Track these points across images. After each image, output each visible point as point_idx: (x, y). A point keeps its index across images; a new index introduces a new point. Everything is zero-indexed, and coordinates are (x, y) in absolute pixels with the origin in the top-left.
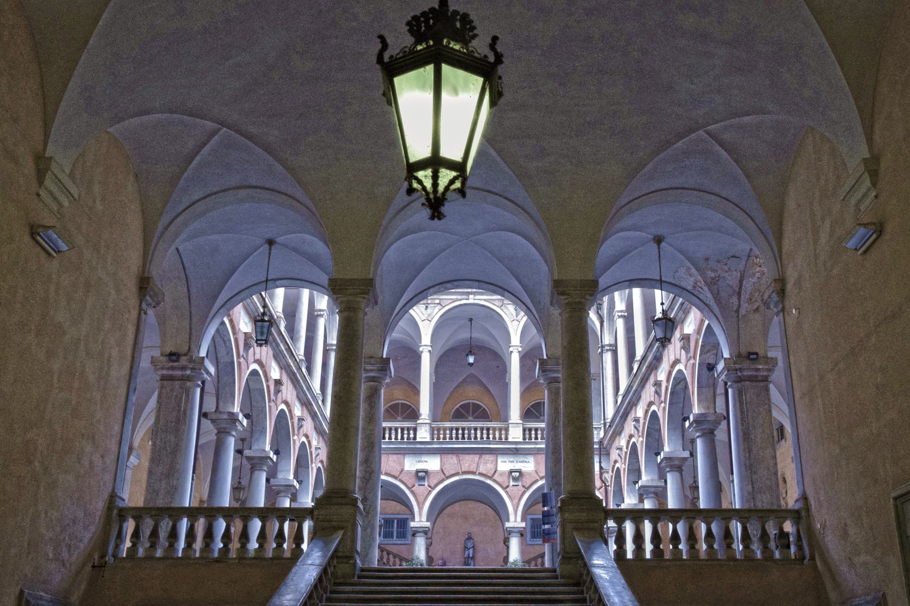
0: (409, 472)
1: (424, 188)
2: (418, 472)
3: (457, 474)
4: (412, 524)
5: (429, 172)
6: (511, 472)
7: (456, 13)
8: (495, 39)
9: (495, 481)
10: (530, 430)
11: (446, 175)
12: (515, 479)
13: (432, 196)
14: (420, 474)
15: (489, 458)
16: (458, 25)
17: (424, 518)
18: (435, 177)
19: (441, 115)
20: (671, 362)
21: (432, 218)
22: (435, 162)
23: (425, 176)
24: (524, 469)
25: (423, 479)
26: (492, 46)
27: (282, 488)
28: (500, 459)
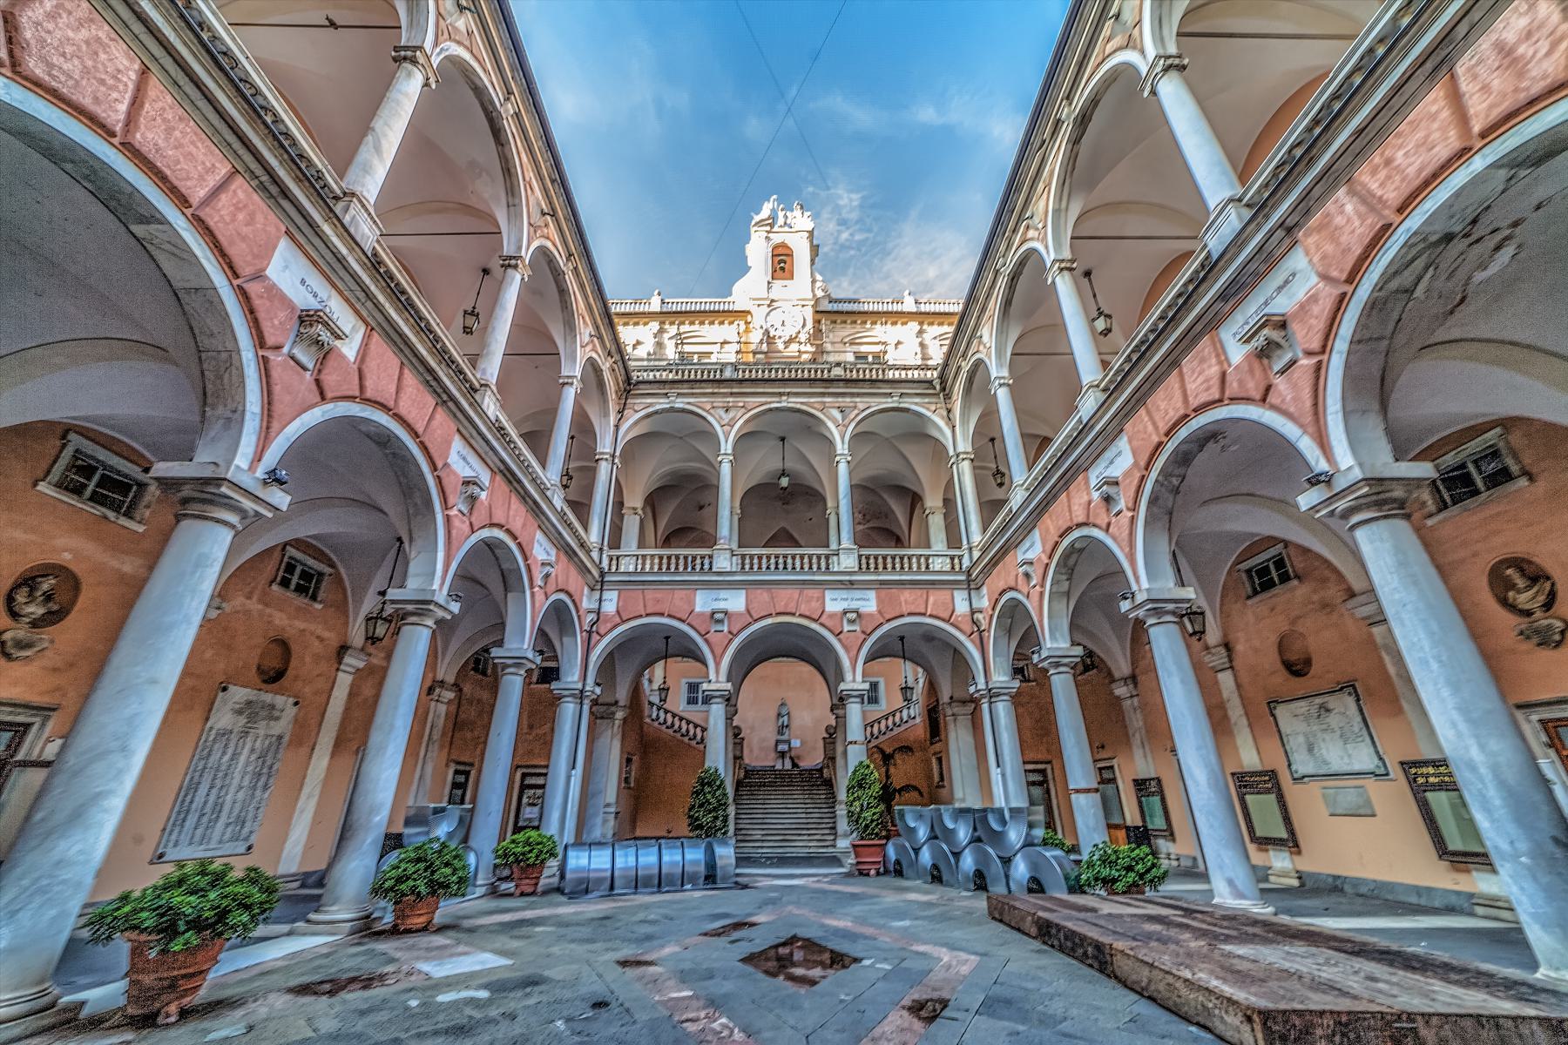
0: (701, 614)
3: (770, 615)
4: (705, 686)
6: (845, 613)
9: (822, 625)
10: (868, 558)
12: (851, 622)
15: (813, 593)
17: (723, 677)
25: (720, 621)
27: (410, 607)
28: (829, 595)
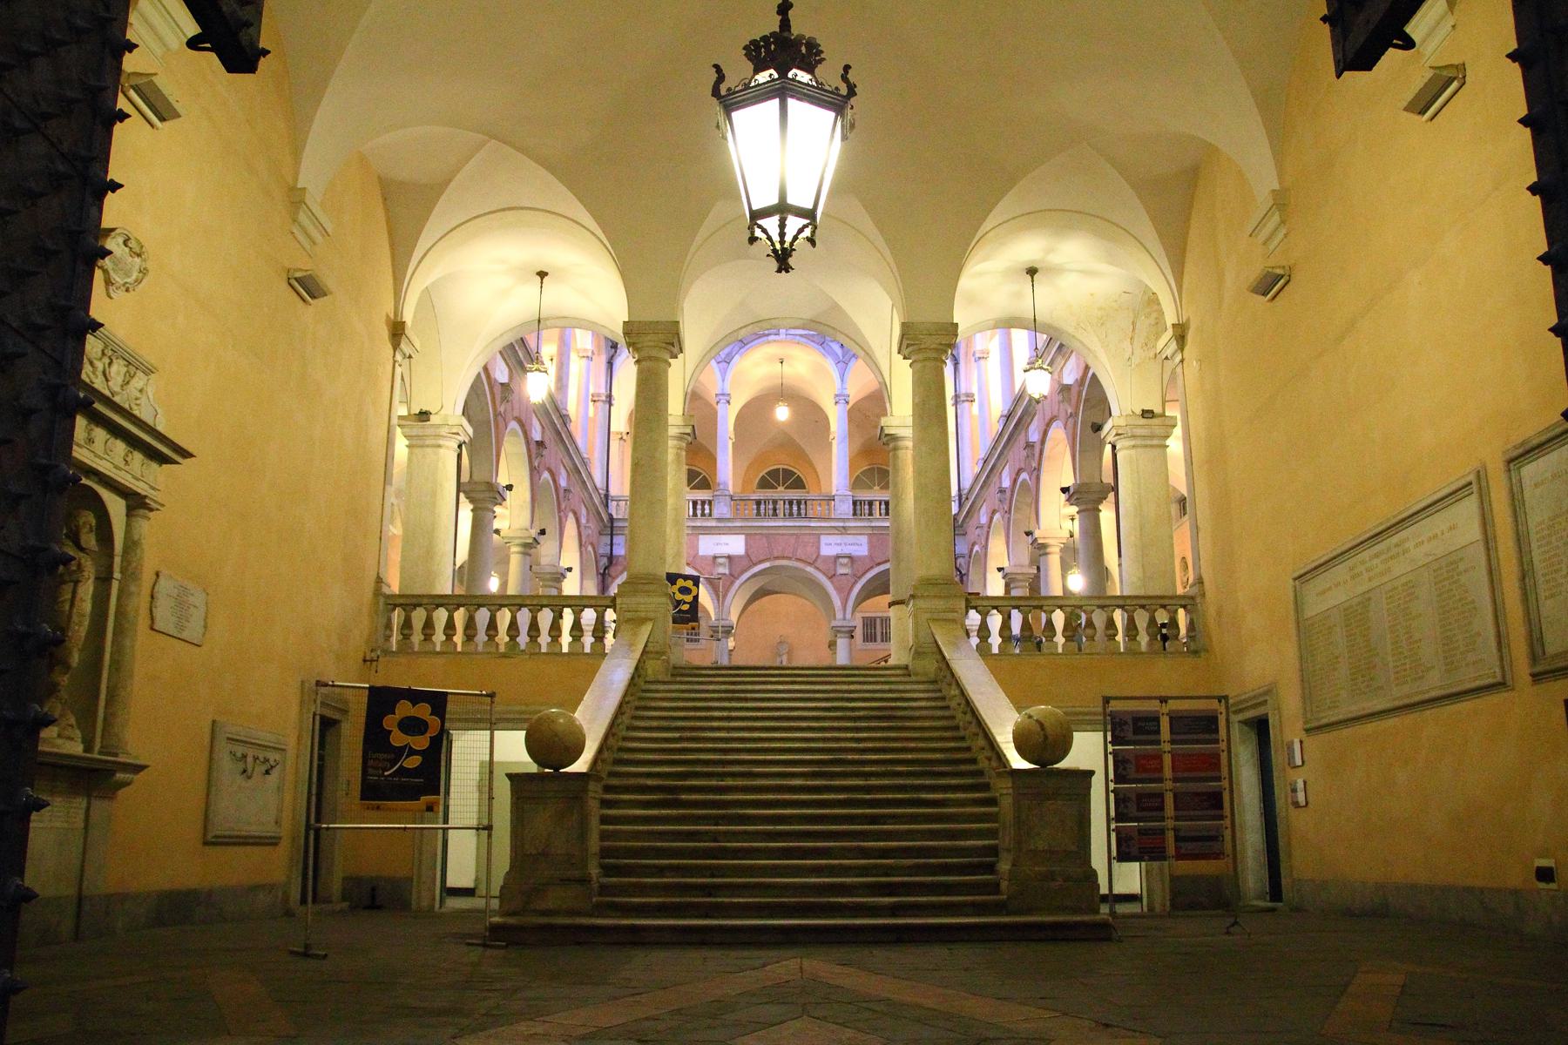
1: (769, 238)
2: (715, 557)
5: (775, 220)
7: (802, 37)
8: (847, 68)
11: (794, 224)
13: (778, 246)
16: (803, 50)
18: (782, 226)
19: (784, 150)
20: (1047, 418)
21: (779, 271)
22: (782, 209)
23: (771, 224)
24: (854, 554)
26: (844, 78)
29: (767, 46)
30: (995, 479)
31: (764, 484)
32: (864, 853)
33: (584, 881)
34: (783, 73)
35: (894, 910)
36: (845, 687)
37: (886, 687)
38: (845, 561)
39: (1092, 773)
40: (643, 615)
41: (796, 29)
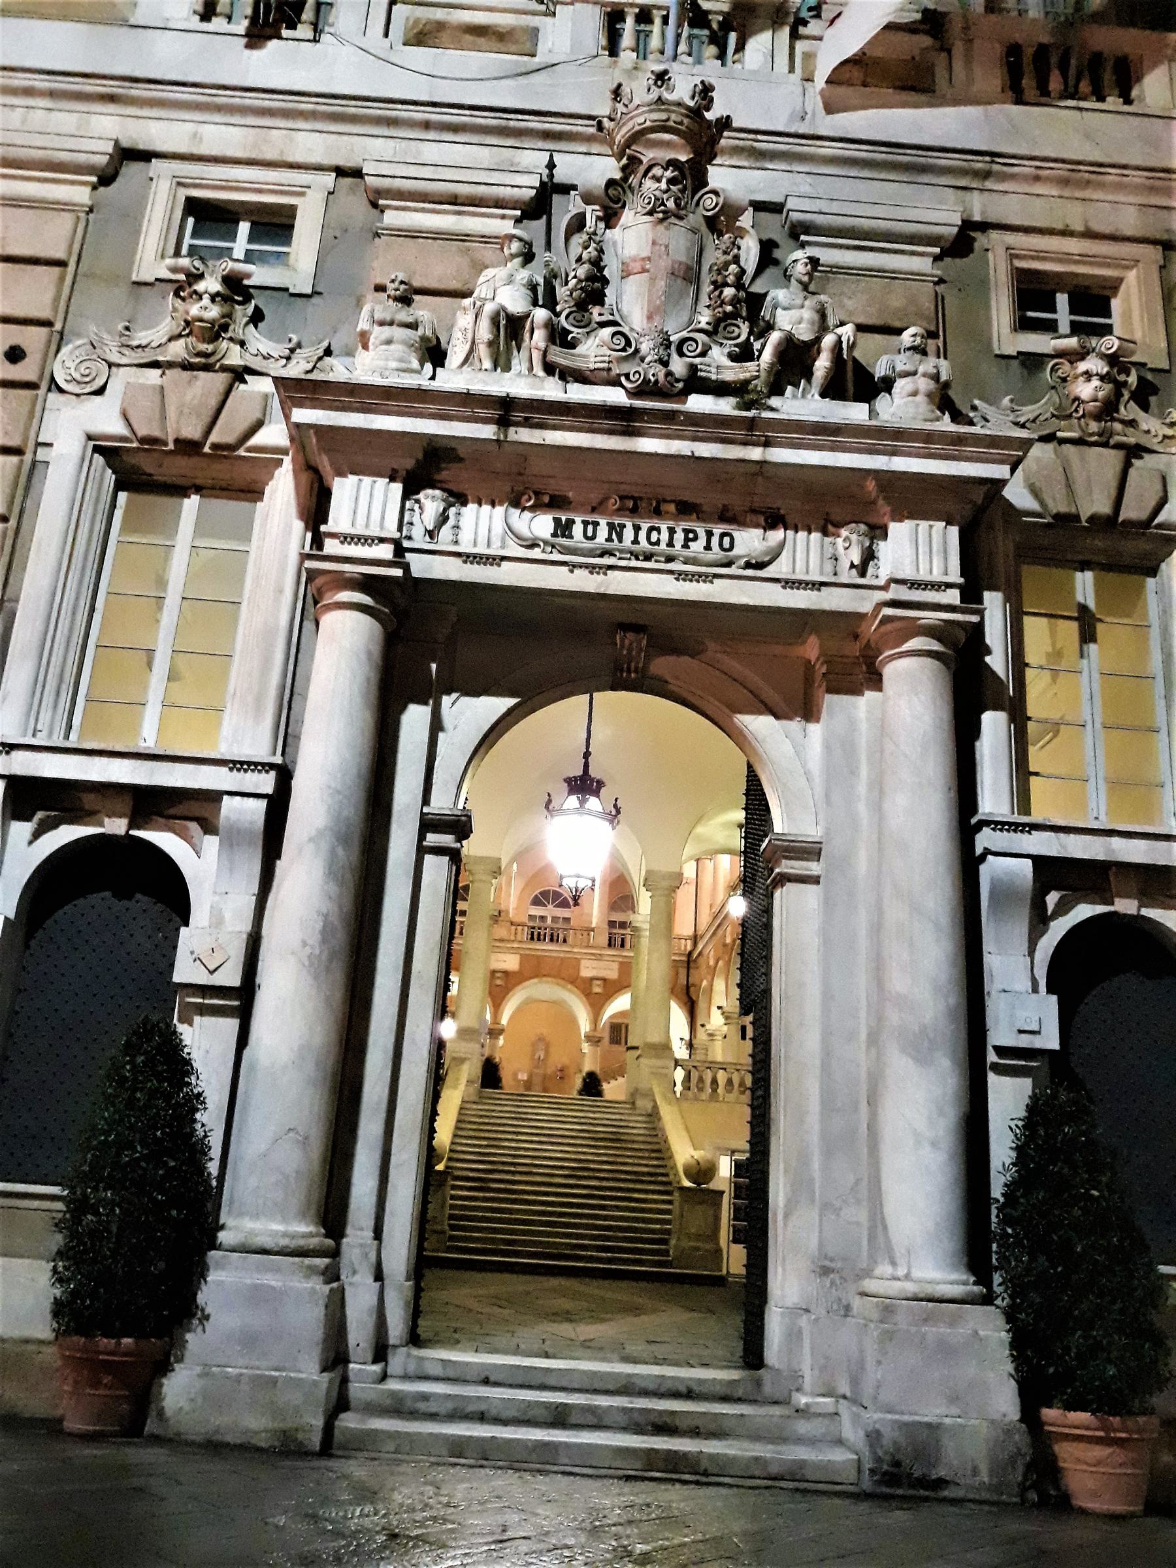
14: (498, 975)
26: (615, 806)
29: (576, 781)
30: (720, 932)
31: (536, 902)
32: (596, 1227)
33: (443, 1232)
34: (582, 802)
35: (610, 1261)
36: (591, 1115)
37: (618, 1117)
38: (599, 982)
39: (723, 1192)
40: (463, 1056)
41: (593, 772)
